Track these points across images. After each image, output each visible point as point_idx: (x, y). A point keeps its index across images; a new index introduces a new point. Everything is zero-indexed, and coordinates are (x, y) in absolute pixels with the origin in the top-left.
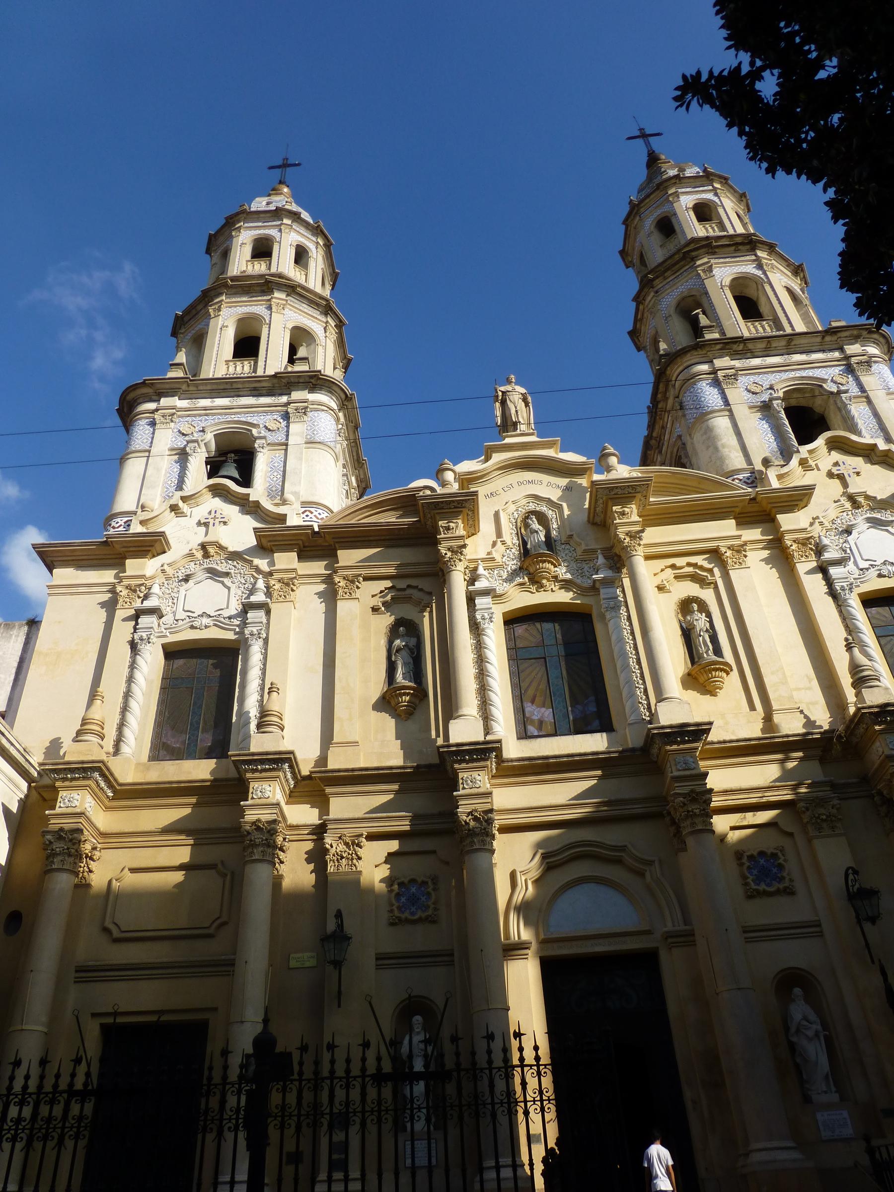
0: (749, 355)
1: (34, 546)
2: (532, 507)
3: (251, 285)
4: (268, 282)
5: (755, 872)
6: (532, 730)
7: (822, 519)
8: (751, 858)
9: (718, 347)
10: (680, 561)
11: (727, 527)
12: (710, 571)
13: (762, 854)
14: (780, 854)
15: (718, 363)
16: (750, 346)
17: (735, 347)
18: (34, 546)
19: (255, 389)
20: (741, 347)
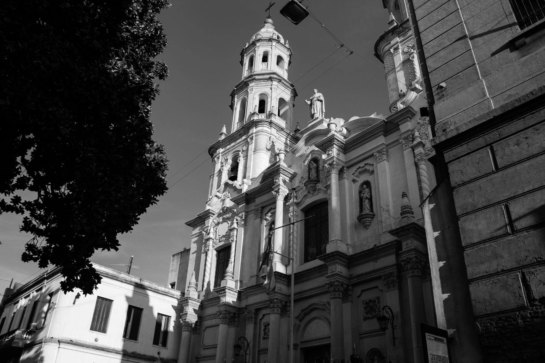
0: (407, 30)
1: (186, 224)
2: (314, 156)
3: (242, 86)
4: (246, 82)
5: (368, 309)
6: (310, 258)
7: (419, 121)
8: (366, 303)
9: (390, 34)
10: (362, 165)
11: (381, 140)
12: (373, 165)
13: (370, 301)
14: (377, 301)
15: (393, 42)
16: (405, 26)
17: (398, 30)
18: (186, 224)
19: (240, 135)
20: (401, 28)
